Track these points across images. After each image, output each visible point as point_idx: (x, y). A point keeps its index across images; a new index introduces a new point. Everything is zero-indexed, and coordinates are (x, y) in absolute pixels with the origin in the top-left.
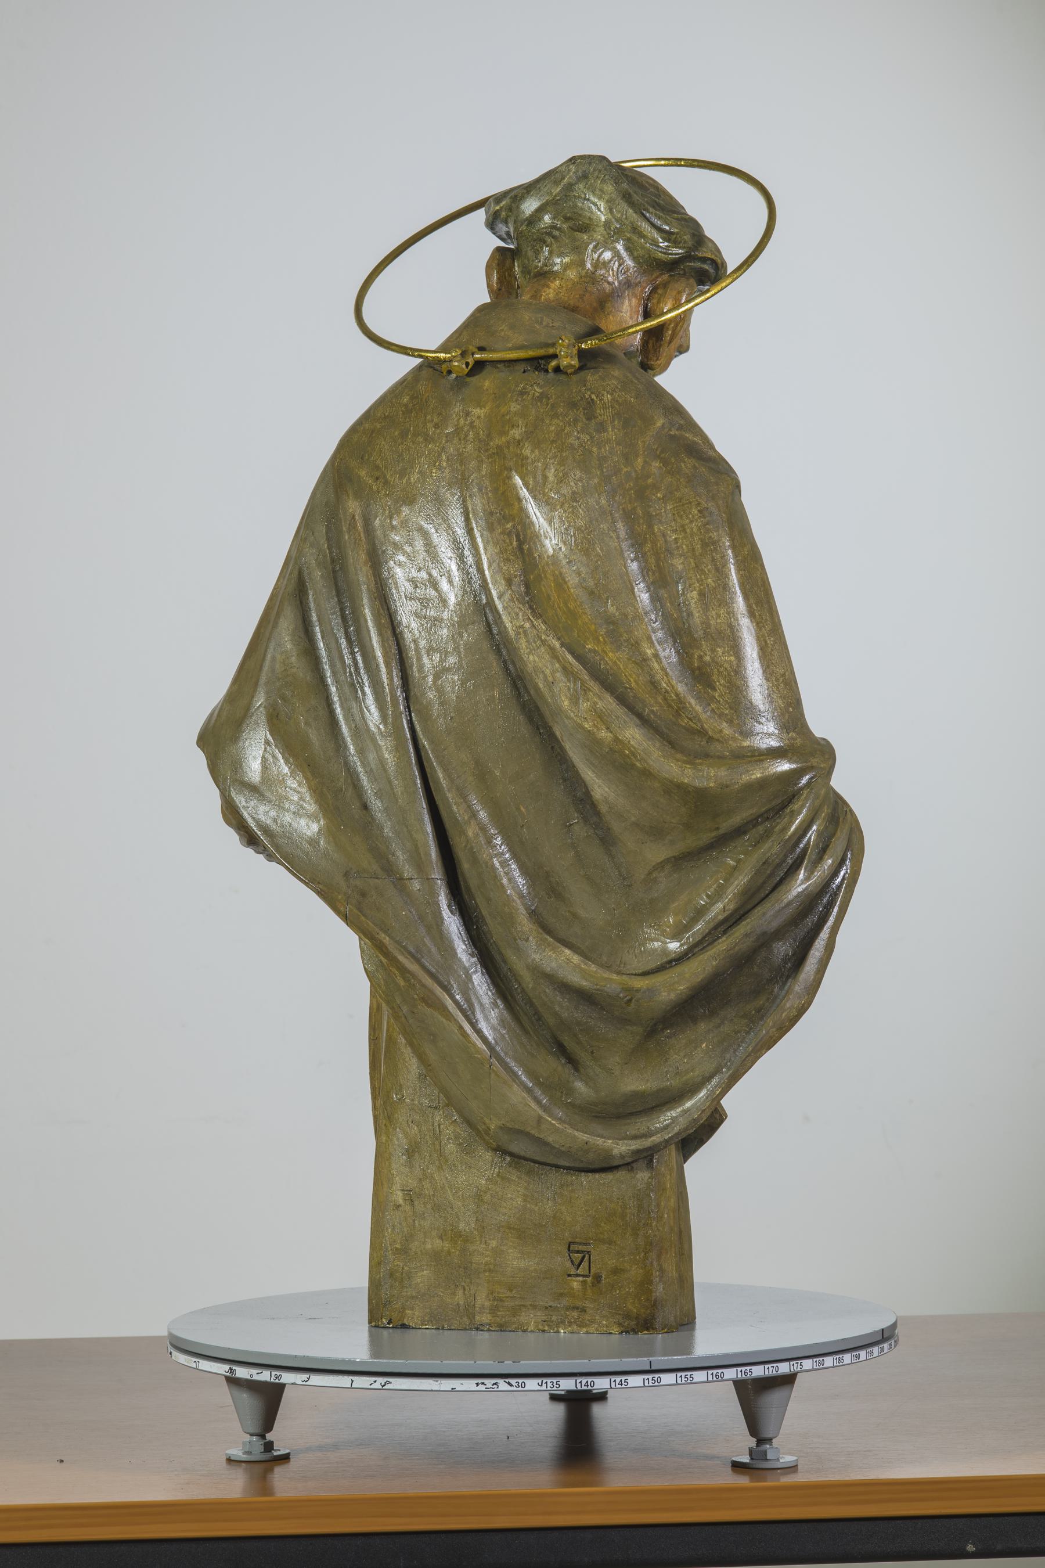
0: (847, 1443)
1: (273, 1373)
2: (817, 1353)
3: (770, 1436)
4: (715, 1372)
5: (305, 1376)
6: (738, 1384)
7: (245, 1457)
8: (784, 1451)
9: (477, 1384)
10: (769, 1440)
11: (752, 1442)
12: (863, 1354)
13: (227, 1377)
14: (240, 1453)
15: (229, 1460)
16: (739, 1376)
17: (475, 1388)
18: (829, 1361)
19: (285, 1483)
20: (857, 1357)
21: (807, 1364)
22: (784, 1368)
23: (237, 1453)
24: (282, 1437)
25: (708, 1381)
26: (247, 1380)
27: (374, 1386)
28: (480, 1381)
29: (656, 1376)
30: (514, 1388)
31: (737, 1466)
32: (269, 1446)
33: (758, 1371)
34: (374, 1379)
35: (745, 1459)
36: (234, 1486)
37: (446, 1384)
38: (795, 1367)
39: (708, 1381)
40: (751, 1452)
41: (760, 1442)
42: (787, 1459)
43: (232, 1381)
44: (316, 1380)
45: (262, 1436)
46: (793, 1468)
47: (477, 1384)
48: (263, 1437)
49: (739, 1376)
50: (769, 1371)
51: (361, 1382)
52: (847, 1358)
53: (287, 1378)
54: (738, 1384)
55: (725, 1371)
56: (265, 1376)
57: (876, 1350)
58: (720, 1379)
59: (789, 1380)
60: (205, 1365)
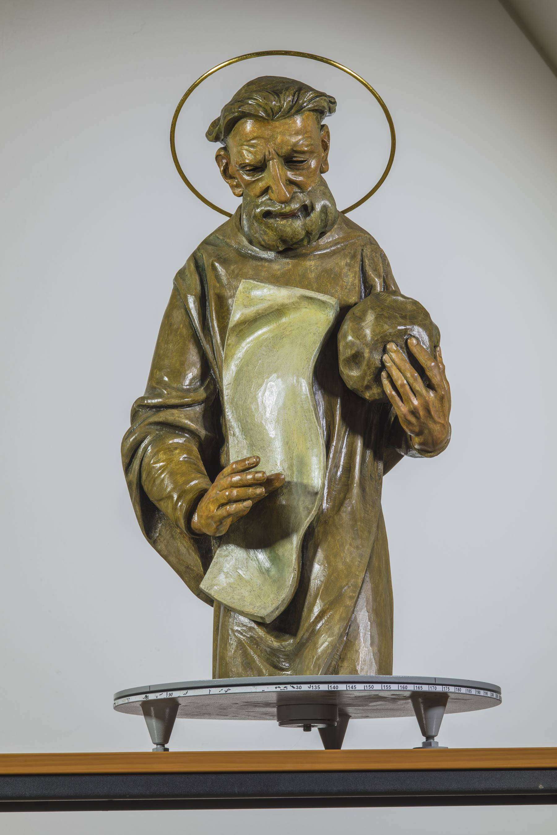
1: (168, 693)
5: (185, 692)
9: (276, 688)
16: (415, 689)
17: (275, 690)
22: (439, 689)
27: (222, 692)
28: (277, 686)
34: (221, 688)
37: (259, 689)
47: (276, 688)
49: (415, 689)
50: (432, 689)
51: (215, 691)
53: (175, 694)
56: (164, 695)
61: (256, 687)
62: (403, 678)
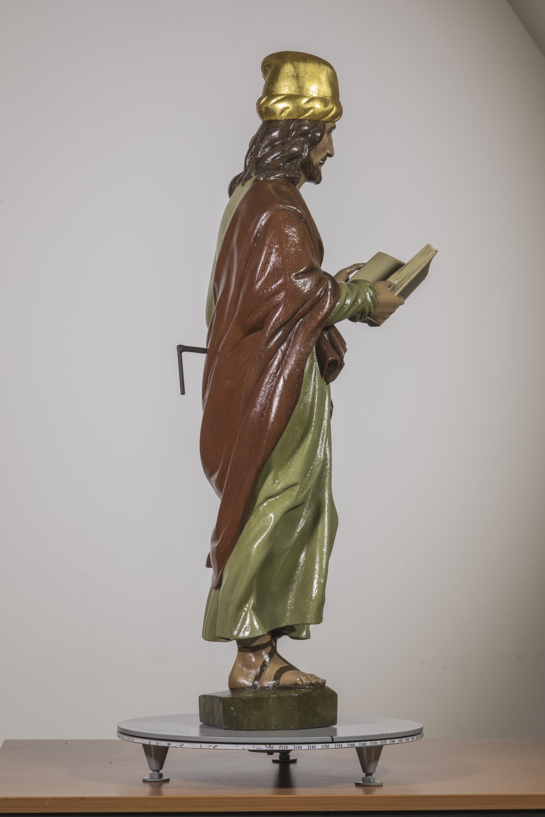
0: (402, 777)
2: (393, 737)
3: (371, 772)
4: (351, 743)
6: (359, 750)
7: (152, 780)
8: (377, 777)
10: (371, 774)
11: (364, 775)
12: (410, 739)
13: (144, 746)
14: (149, 778)
15: (144, 781)
18: (397, 741)
19: (168, 791)
20: (408, 740)
21: (388, 742)
22: (379, 743)
23: (147, 778)
24: (166, 771)
25: (348, 747)
26: (154, 746)
29: (327, 744)
30: (269, 749)
31: (357, 785)
32: (161, 776)
33: (368, 744)
35: (361, 782)
36: (145, 791)
38: (383, 742)
39: (348, 747)
40: (363, 779)
41: (367, 775)
42: (378, 782)
43: (146, 747)
44: (186, 745)
45: (158, 771)
46: (381, 785)
48: (158, 771)
52: (404, 740)
54: (359, 750)
55: (355, 743)
57: (415, 737)
58: (353, 746)
59: (379, 749)
60: (136, 740)
61: (238, 745)
62: (352, 737)
